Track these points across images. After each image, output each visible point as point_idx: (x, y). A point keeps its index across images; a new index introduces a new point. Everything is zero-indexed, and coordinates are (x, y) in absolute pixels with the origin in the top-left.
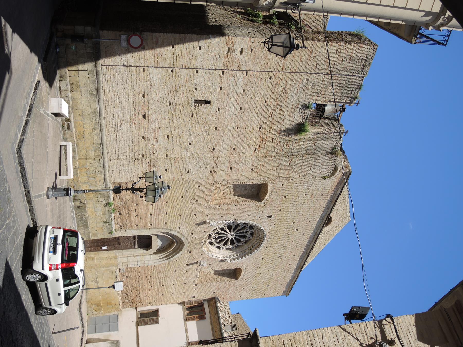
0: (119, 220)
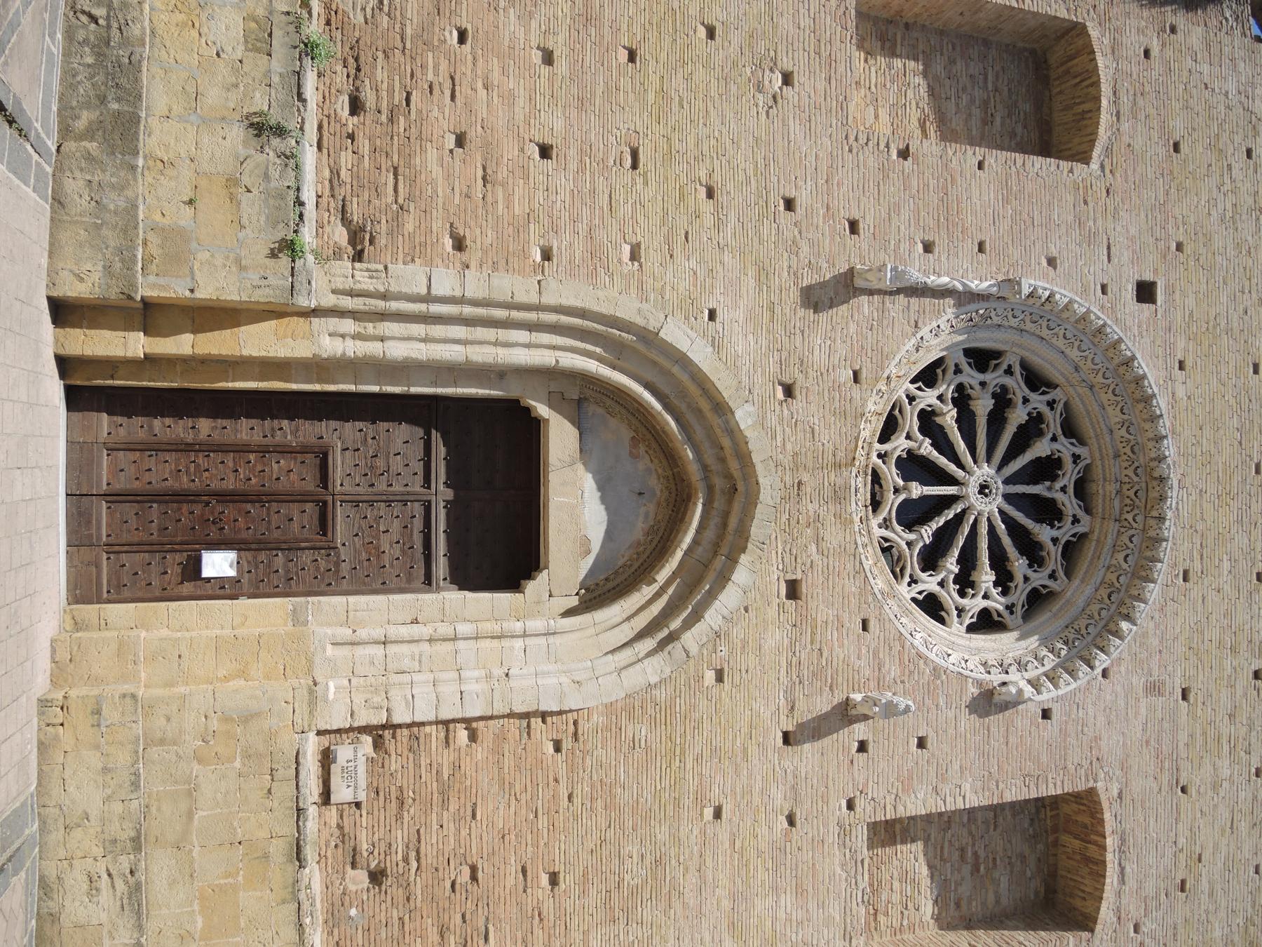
0: (346, 159)
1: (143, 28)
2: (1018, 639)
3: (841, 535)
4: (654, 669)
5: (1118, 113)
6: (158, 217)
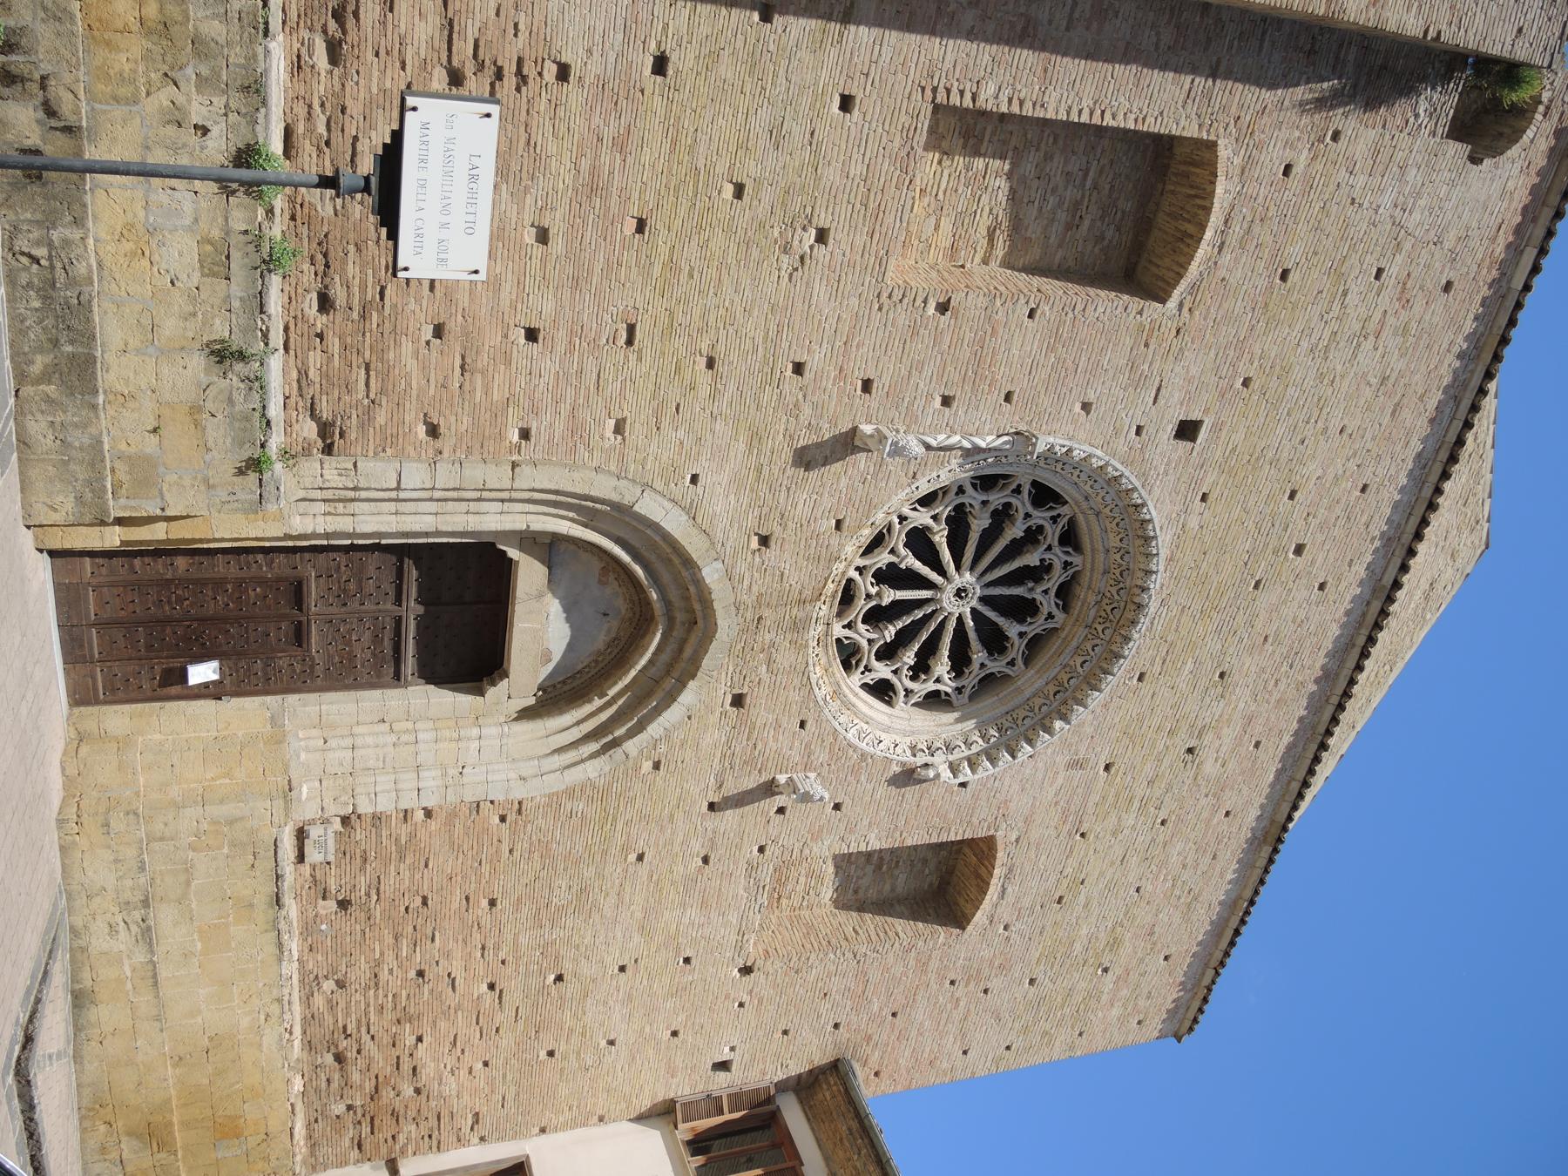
0: (315, 359)
1: (89, 266)
2: (958, 721)
3: (793, 658)
4: (593, 770)
5: (1223, 243)
6: (123, 447)
